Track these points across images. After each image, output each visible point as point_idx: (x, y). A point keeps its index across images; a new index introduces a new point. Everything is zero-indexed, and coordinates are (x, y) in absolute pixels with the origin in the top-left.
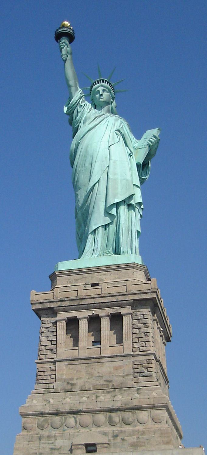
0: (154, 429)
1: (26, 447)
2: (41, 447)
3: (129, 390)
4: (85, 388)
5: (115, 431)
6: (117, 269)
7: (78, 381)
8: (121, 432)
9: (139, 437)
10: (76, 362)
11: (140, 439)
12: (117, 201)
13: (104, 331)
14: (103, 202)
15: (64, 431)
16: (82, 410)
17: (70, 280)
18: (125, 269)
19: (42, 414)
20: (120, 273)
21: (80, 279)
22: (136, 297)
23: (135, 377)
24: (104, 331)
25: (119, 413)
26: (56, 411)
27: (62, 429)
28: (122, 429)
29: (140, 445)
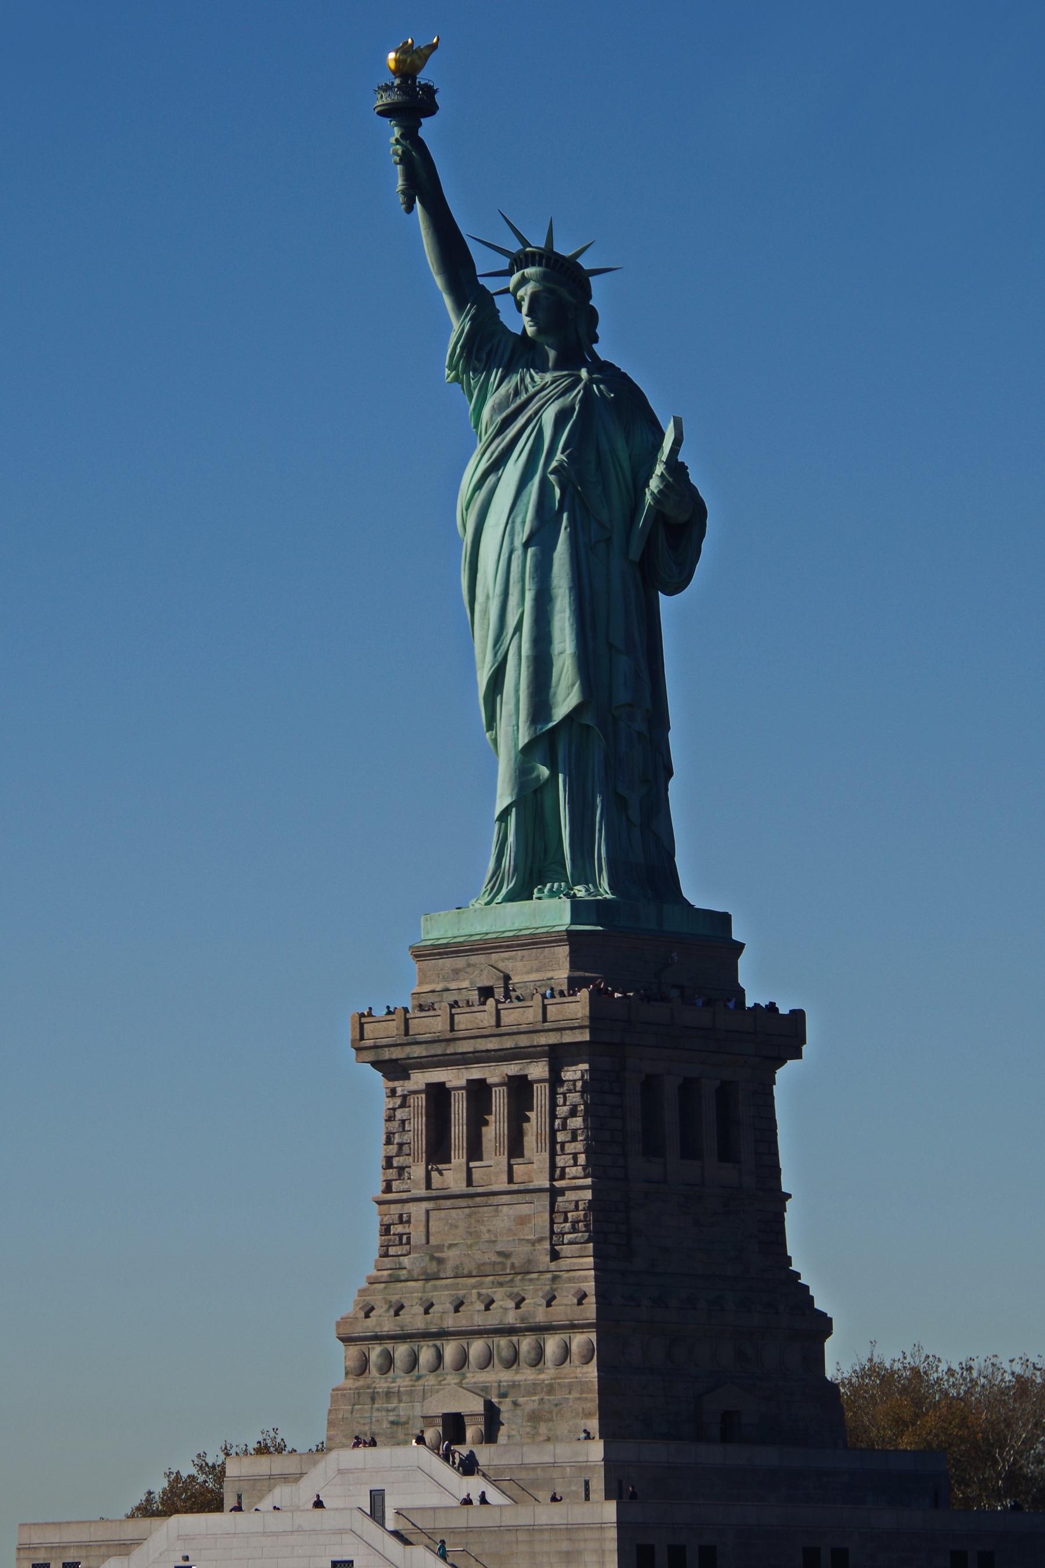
1: (346, 1418)
2: (374, 1419)
8: (515, 1385)
9: (542, 1399)
10: (448, 1203)
11: (544, 1403)
15: (419, 1378)
16: (446, 1329)
19: (378, 1338)
21: (464, 968)
22: (552, 1039)
25: (515, 1339)
26: (401, 1332)
27: (416, 1374)
28: (518, 1378)
29: (543, 1417)
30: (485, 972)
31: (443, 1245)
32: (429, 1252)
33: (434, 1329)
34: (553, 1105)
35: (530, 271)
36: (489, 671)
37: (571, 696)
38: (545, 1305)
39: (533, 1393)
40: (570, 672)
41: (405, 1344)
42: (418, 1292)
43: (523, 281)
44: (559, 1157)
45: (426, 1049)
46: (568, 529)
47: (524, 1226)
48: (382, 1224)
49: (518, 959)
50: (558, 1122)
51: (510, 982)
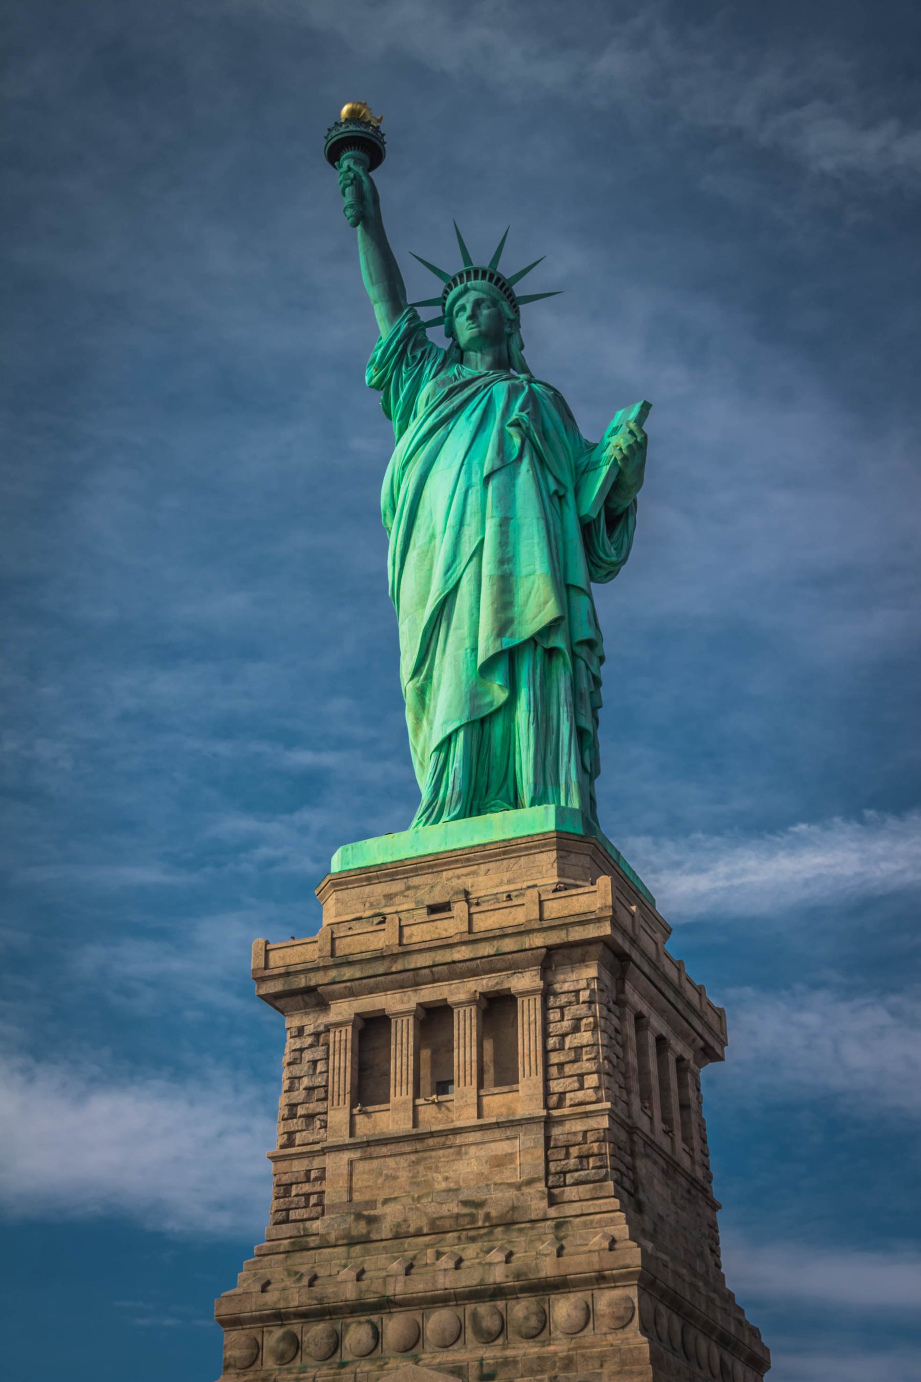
0: (599, 1350)
3: (532, 1228)
4: (406, 1229)
5: (488, 1361)
6: (504, 853)
7: (389, 1209)
8: (507, 1363)
9: (556, 1377)
10: (384, 1150)
12: (508, 642)
13: (462, 1050)
14: (468, 651)
15: (343, 1365)
16: (392, 1298)
17: (372, 899)
18: (527, 853)
19: (280, 1317)
20: (516, 867)
21: (401, 893)
22: (555, 938)
23: (554, 1187)
24: (462, 1050)
25: (501, 1304)
26: (319, 1306)
27: (338, 1361)
28: (509, 1353)
30: (438, 888)
31: (376, 1201)
32: (352, 1211)
33: (371, 1298)
34: (546, 1022)
35: (472, 283)
36: (436, 601)
37: (543, 613)
38: (556, 1255)
39: (539, 1371)
40: (541, 591)
41: (321, 1322)
42: (339, 1259)
43: (466, 290)
44: (555, 1082)
45: (361, 970)
46: (531, 472)
47: (501, 1168)
48: (279, 1183)
49: (482, 872)
50: (552, 1042)
51: (471, 897)
